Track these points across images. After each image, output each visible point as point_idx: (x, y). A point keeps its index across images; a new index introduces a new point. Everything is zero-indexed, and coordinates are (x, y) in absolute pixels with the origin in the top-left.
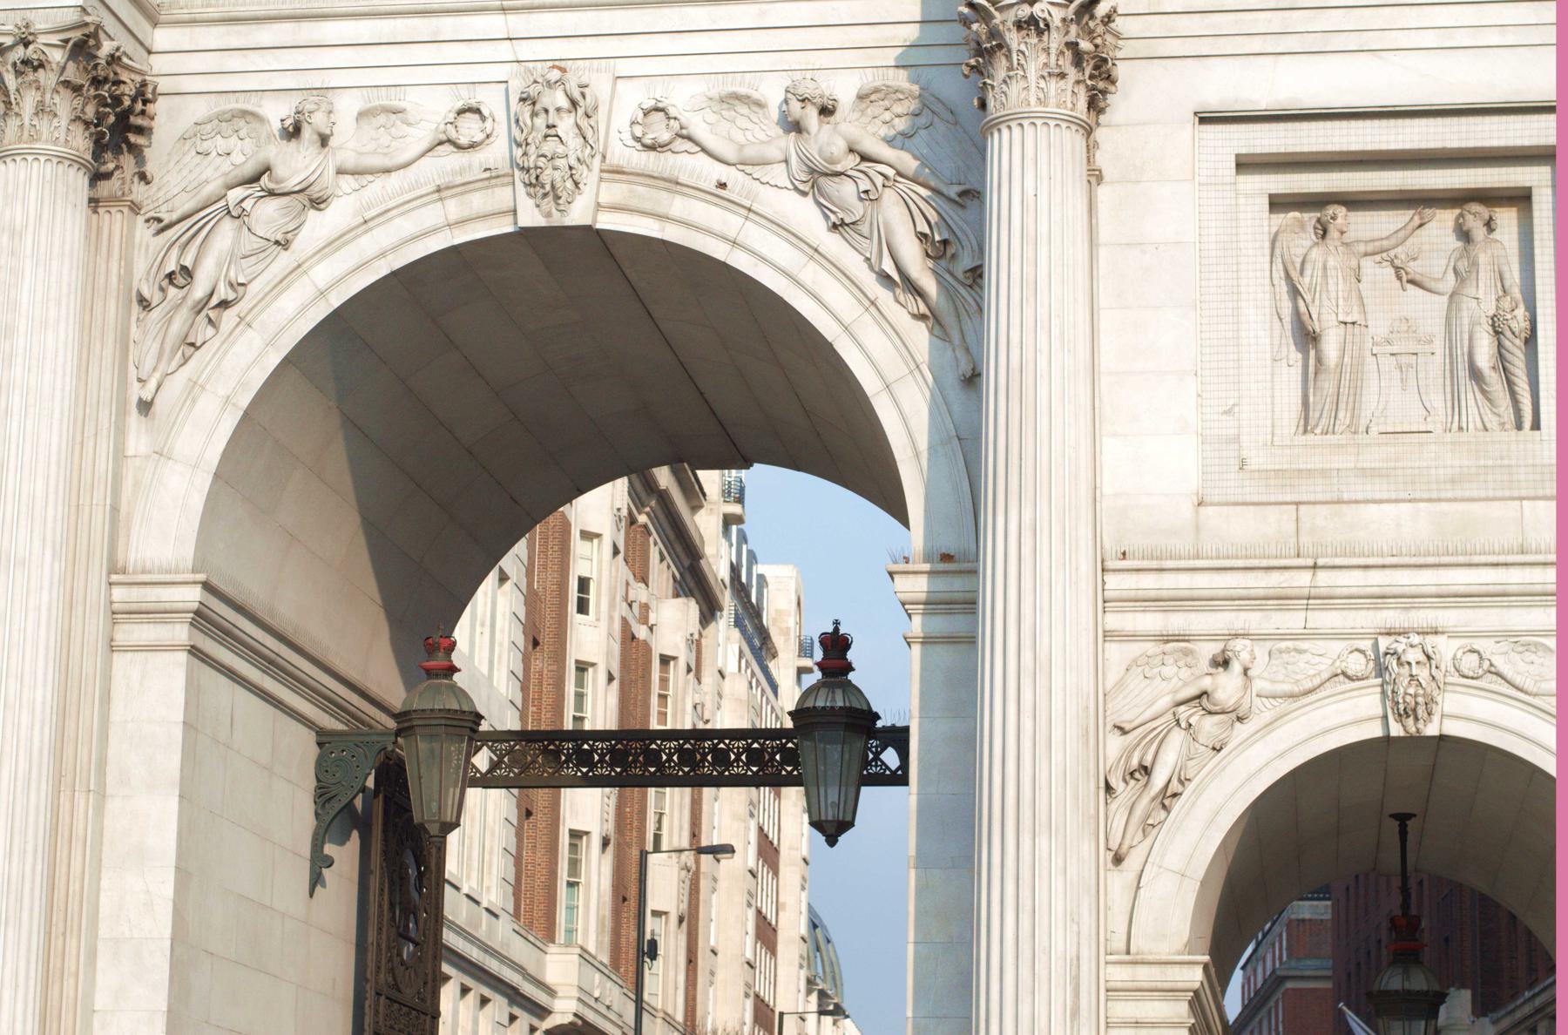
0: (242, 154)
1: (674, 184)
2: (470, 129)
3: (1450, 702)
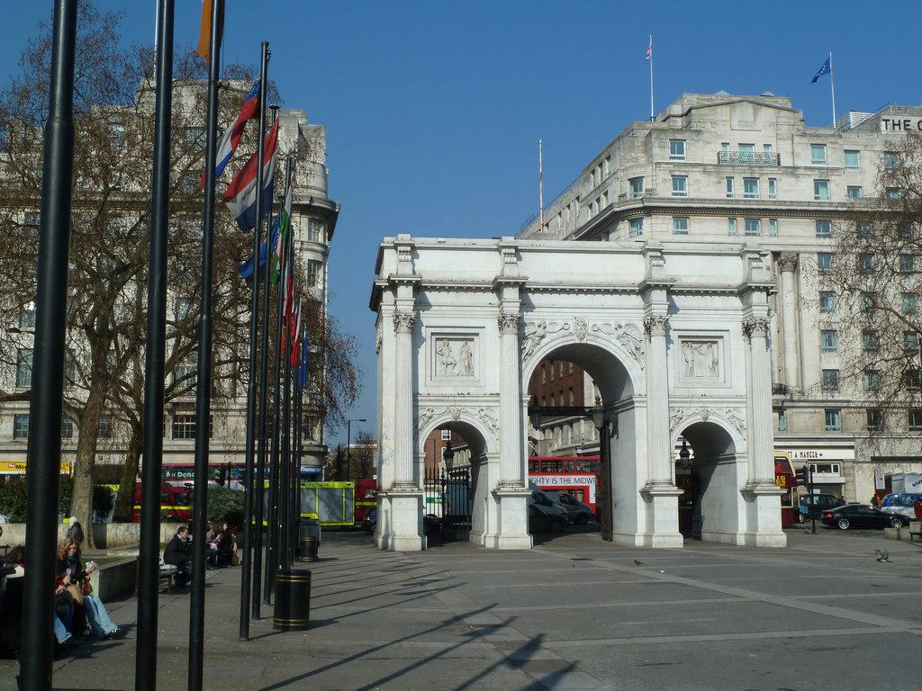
1: (598, 337)
2: (566, 327)
3: (710, 417)
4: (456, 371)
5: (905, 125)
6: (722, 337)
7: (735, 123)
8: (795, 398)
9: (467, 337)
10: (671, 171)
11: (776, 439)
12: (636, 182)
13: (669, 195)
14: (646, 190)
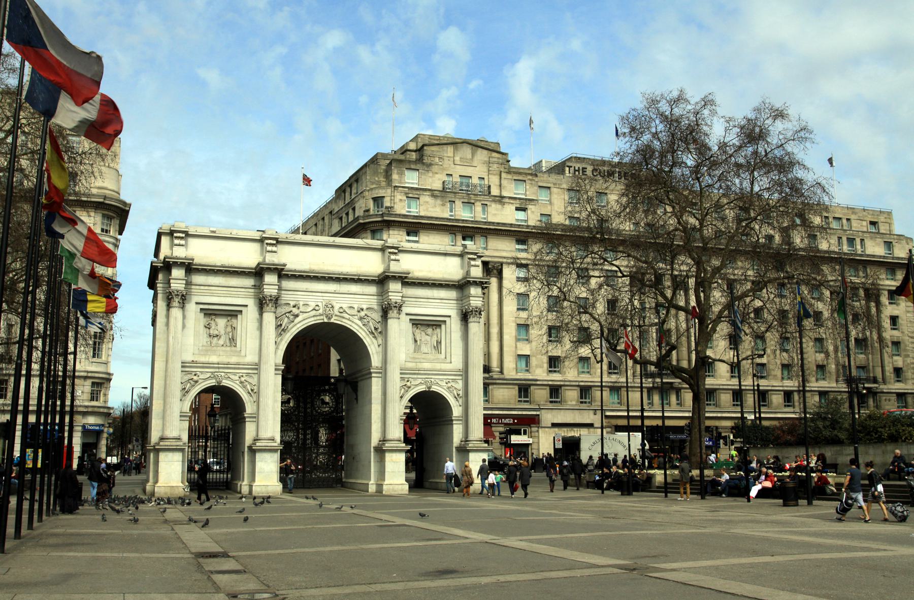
0: (288, 309)
2: (317, 308)
4: (221, 342)
5: (583, 172)
6: (445, 321)
7: (457, 158)
8: (495, 377)
9: (232, 314)
10: (406, 193)
11: (485, 409)
12: (378, 200)
13: (404, 212)
14: (387, 208)
